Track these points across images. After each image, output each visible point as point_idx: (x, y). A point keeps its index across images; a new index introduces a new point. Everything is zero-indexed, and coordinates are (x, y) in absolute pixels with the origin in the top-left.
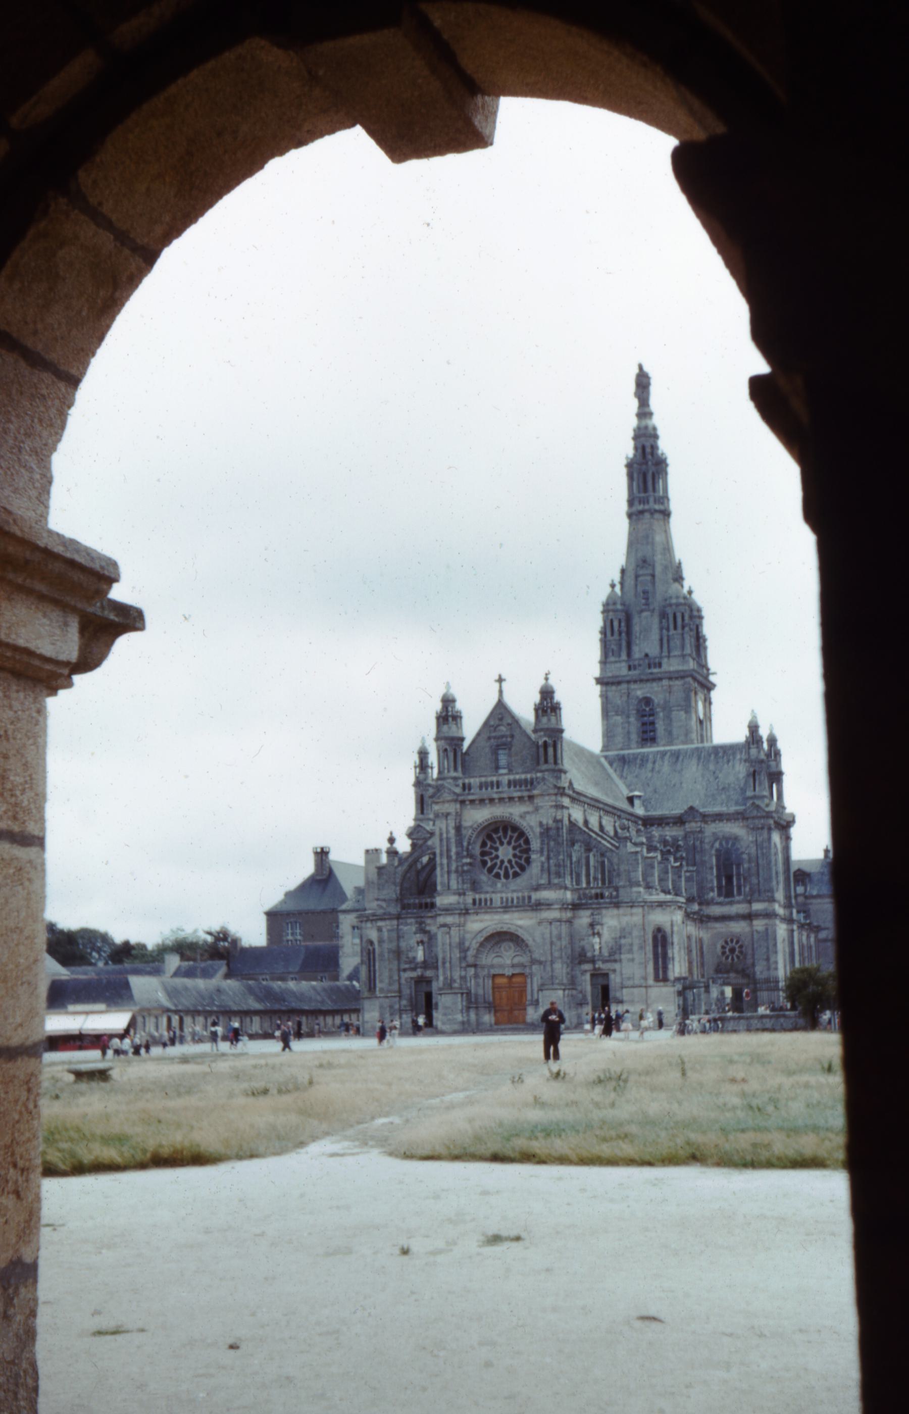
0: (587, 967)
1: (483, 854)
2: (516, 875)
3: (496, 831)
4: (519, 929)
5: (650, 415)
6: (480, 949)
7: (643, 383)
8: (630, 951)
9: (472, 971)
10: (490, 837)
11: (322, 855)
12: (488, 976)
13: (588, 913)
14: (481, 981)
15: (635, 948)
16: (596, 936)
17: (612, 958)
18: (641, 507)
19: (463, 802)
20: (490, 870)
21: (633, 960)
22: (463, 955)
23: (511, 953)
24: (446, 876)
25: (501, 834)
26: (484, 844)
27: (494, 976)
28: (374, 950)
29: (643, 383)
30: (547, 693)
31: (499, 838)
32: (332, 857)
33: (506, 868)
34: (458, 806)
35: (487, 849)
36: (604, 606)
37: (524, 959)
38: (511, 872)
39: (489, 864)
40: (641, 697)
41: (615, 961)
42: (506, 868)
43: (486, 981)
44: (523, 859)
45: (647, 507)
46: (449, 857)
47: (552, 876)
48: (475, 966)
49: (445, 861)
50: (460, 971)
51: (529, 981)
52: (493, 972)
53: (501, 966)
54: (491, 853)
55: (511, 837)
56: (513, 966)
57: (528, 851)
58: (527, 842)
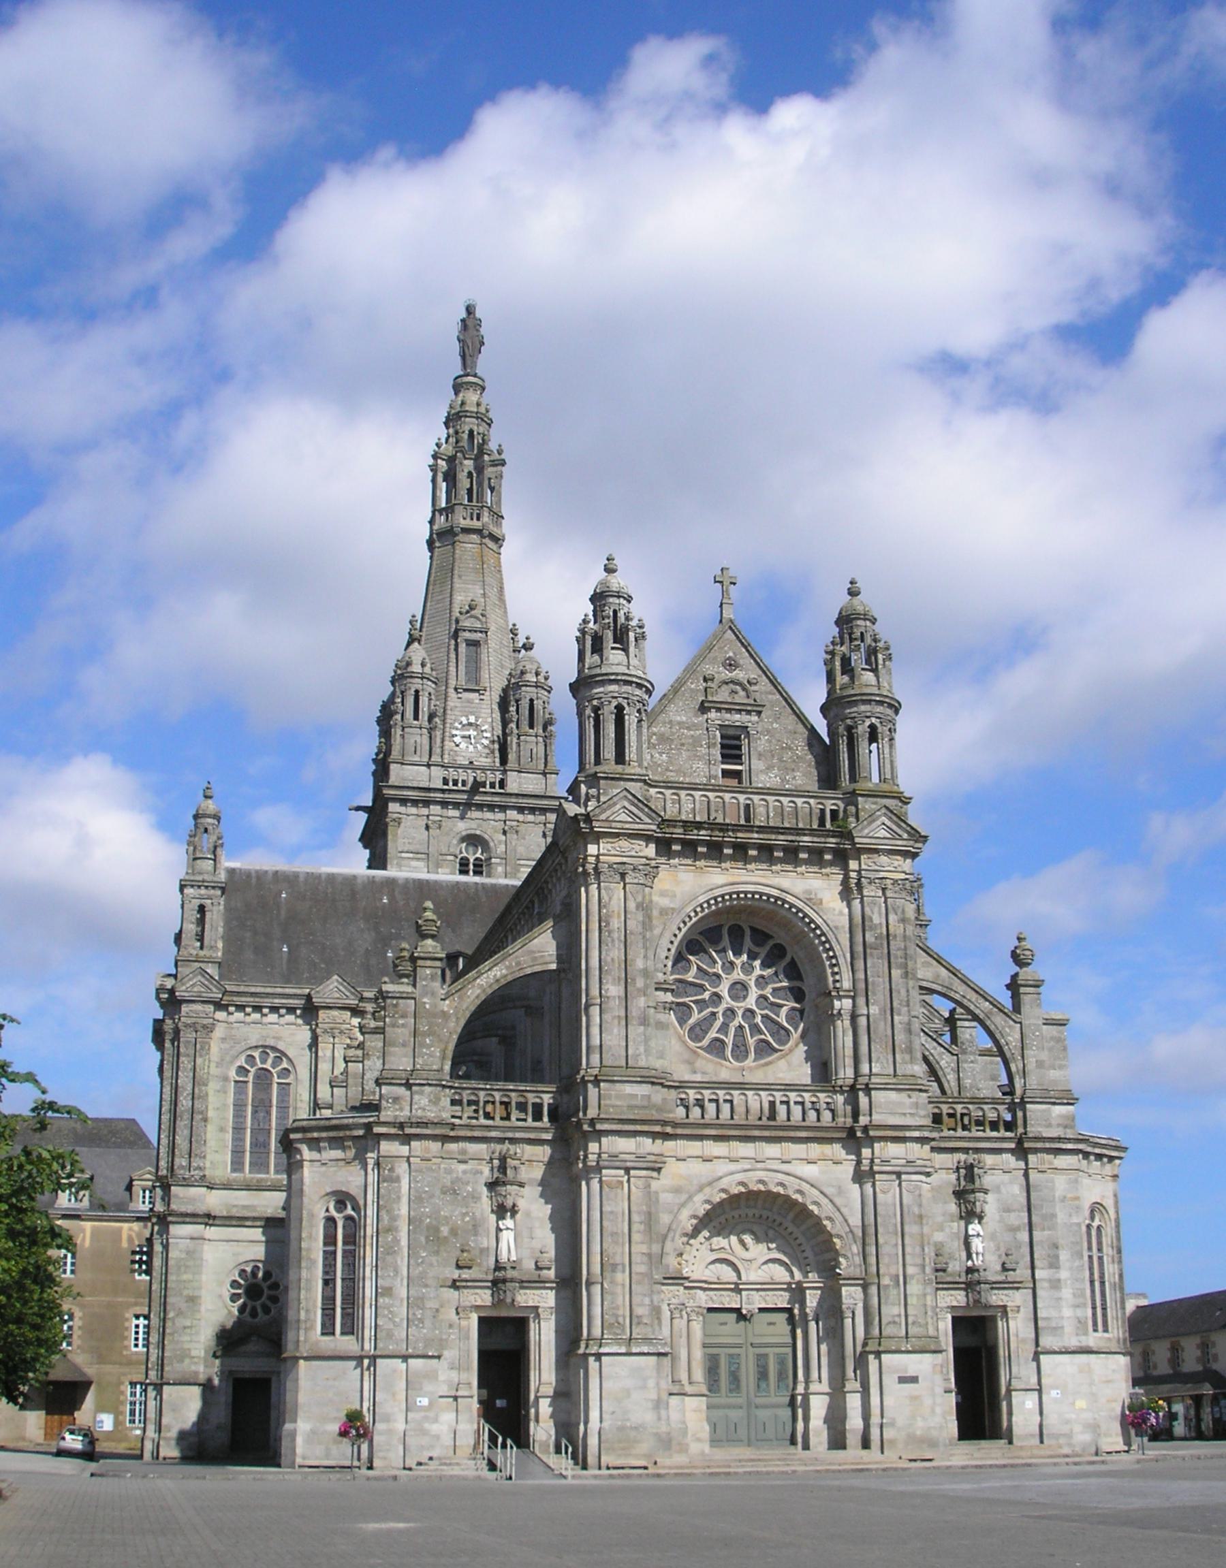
2: (764, 1049)
8: (1054, 1264)
9: (673, 1294)
12: (698, 1310)
15: (1064, 1256)
17: (1011, 1276)
19: (664, 846)
20: (697, 1032)
22: (656, 1248)
25: (726, 941)
34: (651, 850)
38: (752, 1042)
39: (696, 1017)
40: (464, 833)
44: (784, 1011)
45: (476, 524)
49: (614, 990)
54: (702, 988)
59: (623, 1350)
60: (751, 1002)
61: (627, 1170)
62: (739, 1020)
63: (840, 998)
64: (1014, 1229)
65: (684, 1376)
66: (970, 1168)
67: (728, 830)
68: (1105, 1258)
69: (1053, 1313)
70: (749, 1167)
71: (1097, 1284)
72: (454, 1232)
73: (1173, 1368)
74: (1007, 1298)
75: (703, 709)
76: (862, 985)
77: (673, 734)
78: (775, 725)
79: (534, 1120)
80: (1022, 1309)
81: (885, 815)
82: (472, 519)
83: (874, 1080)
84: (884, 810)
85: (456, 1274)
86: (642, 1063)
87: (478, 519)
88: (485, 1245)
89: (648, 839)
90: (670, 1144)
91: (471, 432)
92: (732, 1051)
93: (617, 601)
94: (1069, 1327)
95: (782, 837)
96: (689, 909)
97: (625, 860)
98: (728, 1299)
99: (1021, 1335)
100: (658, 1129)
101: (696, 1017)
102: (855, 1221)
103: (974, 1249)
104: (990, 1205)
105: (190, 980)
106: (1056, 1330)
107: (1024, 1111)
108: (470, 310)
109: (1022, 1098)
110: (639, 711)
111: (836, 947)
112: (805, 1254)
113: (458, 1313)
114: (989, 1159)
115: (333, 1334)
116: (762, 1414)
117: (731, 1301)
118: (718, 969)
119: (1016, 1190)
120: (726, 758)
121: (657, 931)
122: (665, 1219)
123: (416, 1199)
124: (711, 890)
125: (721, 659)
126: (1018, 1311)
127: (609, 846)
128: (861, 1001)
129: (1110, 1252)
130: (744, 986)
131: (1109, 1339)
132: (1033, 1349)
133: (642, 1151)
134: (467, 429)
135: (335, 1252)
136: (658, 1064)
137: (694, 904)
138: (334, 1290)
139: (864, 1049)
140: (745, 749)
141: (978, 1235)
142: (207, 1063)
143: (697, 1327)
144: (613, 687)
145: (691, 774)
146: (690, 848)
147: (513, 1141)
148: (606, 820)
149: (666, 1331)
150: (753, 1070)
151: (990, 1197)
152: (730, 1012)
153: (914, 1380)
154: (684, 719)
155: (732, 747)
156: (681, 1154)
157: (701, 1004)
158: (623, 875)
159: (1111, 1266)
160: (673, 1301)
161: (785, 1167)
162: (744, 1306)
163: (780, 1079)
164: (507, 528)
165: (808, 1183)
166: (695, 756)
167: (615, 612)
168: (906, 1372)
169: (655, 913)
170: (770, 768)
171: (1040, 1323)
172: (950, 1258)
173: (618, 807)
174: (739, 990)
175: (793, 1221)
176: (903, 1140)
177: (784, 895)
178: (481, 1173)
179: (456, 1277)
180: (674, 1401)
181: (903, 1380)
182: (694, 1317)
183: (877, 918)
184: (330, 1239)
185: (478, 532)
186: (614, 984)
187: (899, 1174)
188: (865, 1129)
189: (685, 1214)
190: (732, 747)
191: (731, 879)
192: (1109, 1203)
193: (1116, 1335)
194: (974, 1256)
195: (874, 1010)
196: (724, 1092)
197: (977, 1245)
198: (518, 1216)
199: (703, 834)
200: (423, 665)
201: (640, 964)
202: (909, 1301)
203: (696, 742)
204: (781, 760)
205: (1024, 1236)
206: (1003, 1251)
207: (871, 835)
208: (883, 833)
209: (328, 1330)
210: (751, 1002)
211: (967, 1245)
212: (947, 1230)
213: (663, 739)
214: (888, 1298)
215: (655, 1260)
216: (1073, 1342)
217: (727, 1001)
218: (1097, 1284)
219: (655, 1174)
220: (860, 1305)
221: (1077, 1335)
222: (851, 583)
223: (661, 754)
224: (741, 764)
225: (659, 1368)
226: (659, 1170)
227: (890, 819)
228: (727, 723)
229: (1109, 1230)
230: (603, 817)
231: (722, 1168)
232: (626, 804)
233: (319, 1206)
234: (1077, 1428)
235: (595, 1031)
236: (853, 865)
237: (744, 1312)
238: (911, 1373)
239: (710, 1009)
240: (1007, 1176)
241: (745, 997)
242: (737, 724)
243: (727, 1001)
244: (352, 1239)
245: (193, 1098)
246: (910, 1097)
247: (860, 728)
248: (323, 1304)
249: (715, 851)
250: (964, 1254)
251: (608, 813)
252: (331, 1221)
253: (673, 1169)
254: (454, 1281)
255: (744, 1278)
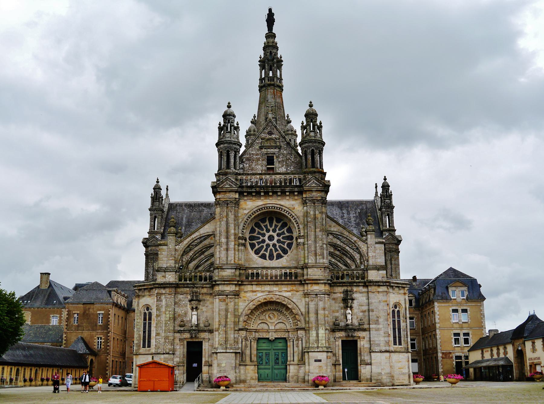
0: (342, 334)
1: (251, 238)
2: (279, 257)
3: (263, 221)
4: (286, 299)
5: (274, 36)
6: (250, 316)
7: (270, 20)
8: (377, 322)
9: (243, 333)
10: (258, 225)
11: (45, 275)
12: (254, 339)
13: (340, 289)
14: (248, 343)
15: (381, 320)
16: (349, 309)
18: (269, 82)
19: (241, 194)
20: (257, 252)
21: (377, 330)
22: (237, 320)
23: (275, 321)
24: (224, 253)
25: (267, 223)
26: (252, 231)
27: (259, 338)
28: (150, 314)
29: (270, 20)
30: (311, 116)
31: (266, 226)
32: (51, 278)
33: (271, 250)
34: (237, 196)
35: (255, 235)
36: (247, 132)
37: (289, 325)
38: (275, 254)
39: (257, 247)
41: (364, 330)
42: (271, 250)
43: (253, 343)
45: (272, 83)
46: (227, 238)
47: (317, 257)
48: (246, 330)
49: (224, 240)
50: (234, 333)
51: (290, 344)
52: (258, 335)
53: (268, 331)
54: (259, 238)
55: (276, 226)
56: (276, 331)
57: (291, 238)
58: (290, 230)
59: (224, 351)
60: (275, 242)
61: (227, 295)
62: (271, 247)
63: (300, 238)
64: (364, 312)
65: (248, 359)
66: (347, 291)
67: (262, 188)
68: (401, 321)
69: (376, 339)
70: (268, 294)
71: (397, 330)
72: (179, 315)
73: (505, 355)
74: (360, 334)
75: (261, 148)
76: (306, 235)
77: (250, 157)
78: (285, 152)
79: (204, 281)
80: (365, 338)
81: (314, 179)
82: (271, 81)
83: (309, 264)
84: (314, 178)
85: (179, 328)
86: (233, 262)
87: (273, 81)
88: (188, 319)
89: (236, 192)
90: (242, 287)
91: (271, 52)
92: (269, 257)
93: (229, 117)
94: (382, 344)
95: (279, 189)
96: (250, 213)
97: (228, 199)
98: (265, 335)
99: (365, 346)
100: (236, 283)
101: (257, 247)
102: (303, 310)
103: (348, 318)
104: (355, 304)
105: (151, 239)
106: (378, 345)
107: (367, 273)
108: (270, 10)
109: (366, 269)
110: (235, 152)
111: (299, 222)
112: (290, 320)
113: (180, 341)
114: (355, 289)
115: (145, 347)
116: (276, 371)
117: (265, 335)
118: (265, 231)
119: (365, 298)
120: (269, 164)
121: (240, 221)
122: (240, 311)
123: (167, 306)
124: (258, 207)
125: (266, 131)
126: (364, 339)
127: (223, 195)
128: (306, 239)
129: (403, 319)
130: (273, 237)
131: (401, 348)
132: (368, 350)
133: (232, 289)
134: (269, 51)
135: (146, 323)
136: (240, 262)
137: (252, 211)
138: (146, 335)
139: (306, 255)
140: (275, 160)
141: (349, 313)
142: (157, 264)
143: (254, 345)
144: (226, 145)
145: (256, 170)
146: (249, 194)
147: (197, 287)
148: (222, 188)
149: (240, 346)
150: (275, 263)
151: (355, 301)
152: (268, 245)
153: (320, 361)
154: (254, 152)
155: (270, 160)
156: (245, 290)
157: (259, 243)
158: (227, 204)
159: (403, 323)
160: (243, 336)
161: (280, 294)
162: (270, 337)
163: (284, 265)
164: (284, 82)
165: (287, 298)
166: (258, 164)
167: (229, 121)
168: (317, 358)
169: (240, 215)
170: (282, 166)
171: (371, 343)
172: (341, 321)
173: (225, 183)
174: (271, 238)
175: (285, 310)
176: (318, 283)
177: (281, 207)
178: (188, 298)
179: (179, 329)
180: (242, 367)
181: (316, 361)
182: (252, 341)
183: (312, 213)
184: (145, 319)
185: (273, 85)
186: (224, 238)
187: (316, 295)
188: (305, 280)
189: (247, 308)
190: (270, 160)
191: (264, 203)
192: (402, 303)
193: (404, 346)
194: (348, 320)
195: (310, 242)
196: (256, 270)
197: (349, 317)
198: (199, 310)
199: (253, 190)
200: (254, 131)
201: (232, 231)
202: (319, 335)
203: (258, 160)
204: (286, 163)
205: (367, 313)
206: (359, 319)
207: (309, 186)
208: (314, 185)
209: (144, 347)
210: (275, 242)
211: (346, 317)
212: (340, 312)
213: (248, 159)
214: (312, 334)
215: (236, 323)
216: (384, 349)
217: (267, 241)
218: (397, 330)
219: (236, 297)
220: (304, 337)
221: (385, 346)
222: (310, 103)
223: (246, 164)
224: (274, 165)
225: (236, 356)
226: (238, 295)
227: (316, 181)
228: (268, 152)
229: (402, 311)
230: (221, 186)
231: (259, 294)
232: (228, 182)
233: (142, 309)
234: (384, 377)
235: (218, 253)
236: (304, 196)
237: (270, 339)
238: (319, 359)
239: (262, 244)
240: (361, 295)
241: (273, 240)
242: (272, 152)
243: (267, 241)
244: (150, 319)
245: (153, 276)
246: (321, 270)
247: (309, 151)
248: (143, 338)
249: (258, 194)
250: (345, 320)
251: (222, 185)
252: (145, 313)
253: (242, 294)
254: (178, 331)
255: (270, 328)
